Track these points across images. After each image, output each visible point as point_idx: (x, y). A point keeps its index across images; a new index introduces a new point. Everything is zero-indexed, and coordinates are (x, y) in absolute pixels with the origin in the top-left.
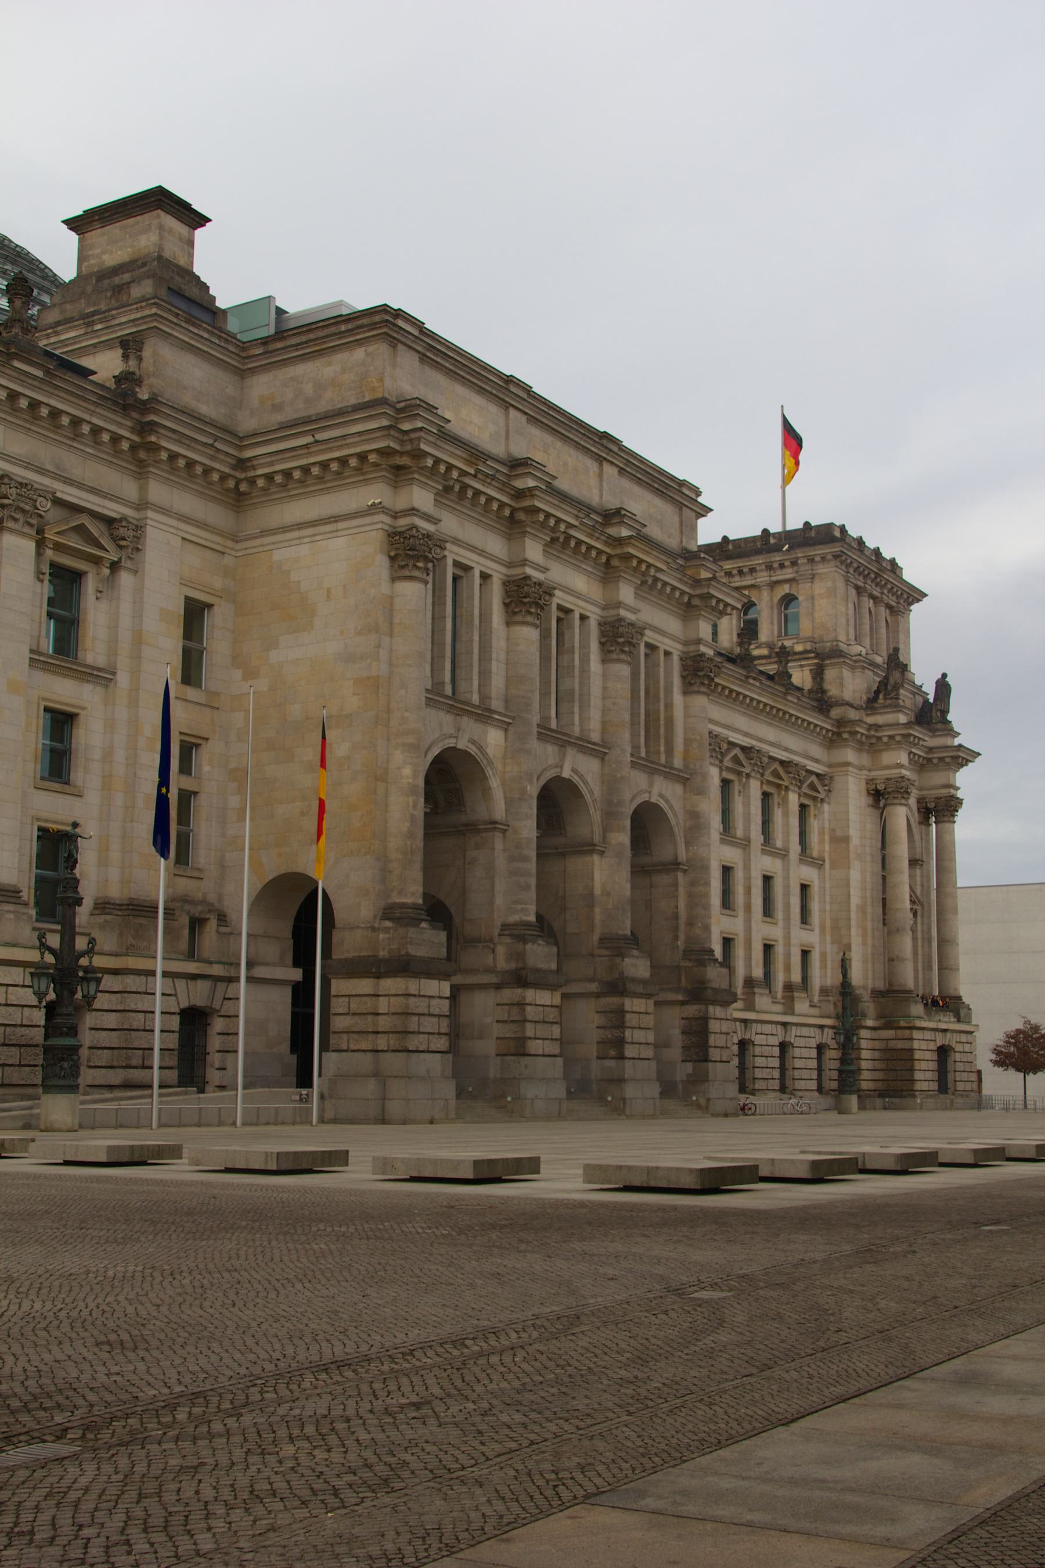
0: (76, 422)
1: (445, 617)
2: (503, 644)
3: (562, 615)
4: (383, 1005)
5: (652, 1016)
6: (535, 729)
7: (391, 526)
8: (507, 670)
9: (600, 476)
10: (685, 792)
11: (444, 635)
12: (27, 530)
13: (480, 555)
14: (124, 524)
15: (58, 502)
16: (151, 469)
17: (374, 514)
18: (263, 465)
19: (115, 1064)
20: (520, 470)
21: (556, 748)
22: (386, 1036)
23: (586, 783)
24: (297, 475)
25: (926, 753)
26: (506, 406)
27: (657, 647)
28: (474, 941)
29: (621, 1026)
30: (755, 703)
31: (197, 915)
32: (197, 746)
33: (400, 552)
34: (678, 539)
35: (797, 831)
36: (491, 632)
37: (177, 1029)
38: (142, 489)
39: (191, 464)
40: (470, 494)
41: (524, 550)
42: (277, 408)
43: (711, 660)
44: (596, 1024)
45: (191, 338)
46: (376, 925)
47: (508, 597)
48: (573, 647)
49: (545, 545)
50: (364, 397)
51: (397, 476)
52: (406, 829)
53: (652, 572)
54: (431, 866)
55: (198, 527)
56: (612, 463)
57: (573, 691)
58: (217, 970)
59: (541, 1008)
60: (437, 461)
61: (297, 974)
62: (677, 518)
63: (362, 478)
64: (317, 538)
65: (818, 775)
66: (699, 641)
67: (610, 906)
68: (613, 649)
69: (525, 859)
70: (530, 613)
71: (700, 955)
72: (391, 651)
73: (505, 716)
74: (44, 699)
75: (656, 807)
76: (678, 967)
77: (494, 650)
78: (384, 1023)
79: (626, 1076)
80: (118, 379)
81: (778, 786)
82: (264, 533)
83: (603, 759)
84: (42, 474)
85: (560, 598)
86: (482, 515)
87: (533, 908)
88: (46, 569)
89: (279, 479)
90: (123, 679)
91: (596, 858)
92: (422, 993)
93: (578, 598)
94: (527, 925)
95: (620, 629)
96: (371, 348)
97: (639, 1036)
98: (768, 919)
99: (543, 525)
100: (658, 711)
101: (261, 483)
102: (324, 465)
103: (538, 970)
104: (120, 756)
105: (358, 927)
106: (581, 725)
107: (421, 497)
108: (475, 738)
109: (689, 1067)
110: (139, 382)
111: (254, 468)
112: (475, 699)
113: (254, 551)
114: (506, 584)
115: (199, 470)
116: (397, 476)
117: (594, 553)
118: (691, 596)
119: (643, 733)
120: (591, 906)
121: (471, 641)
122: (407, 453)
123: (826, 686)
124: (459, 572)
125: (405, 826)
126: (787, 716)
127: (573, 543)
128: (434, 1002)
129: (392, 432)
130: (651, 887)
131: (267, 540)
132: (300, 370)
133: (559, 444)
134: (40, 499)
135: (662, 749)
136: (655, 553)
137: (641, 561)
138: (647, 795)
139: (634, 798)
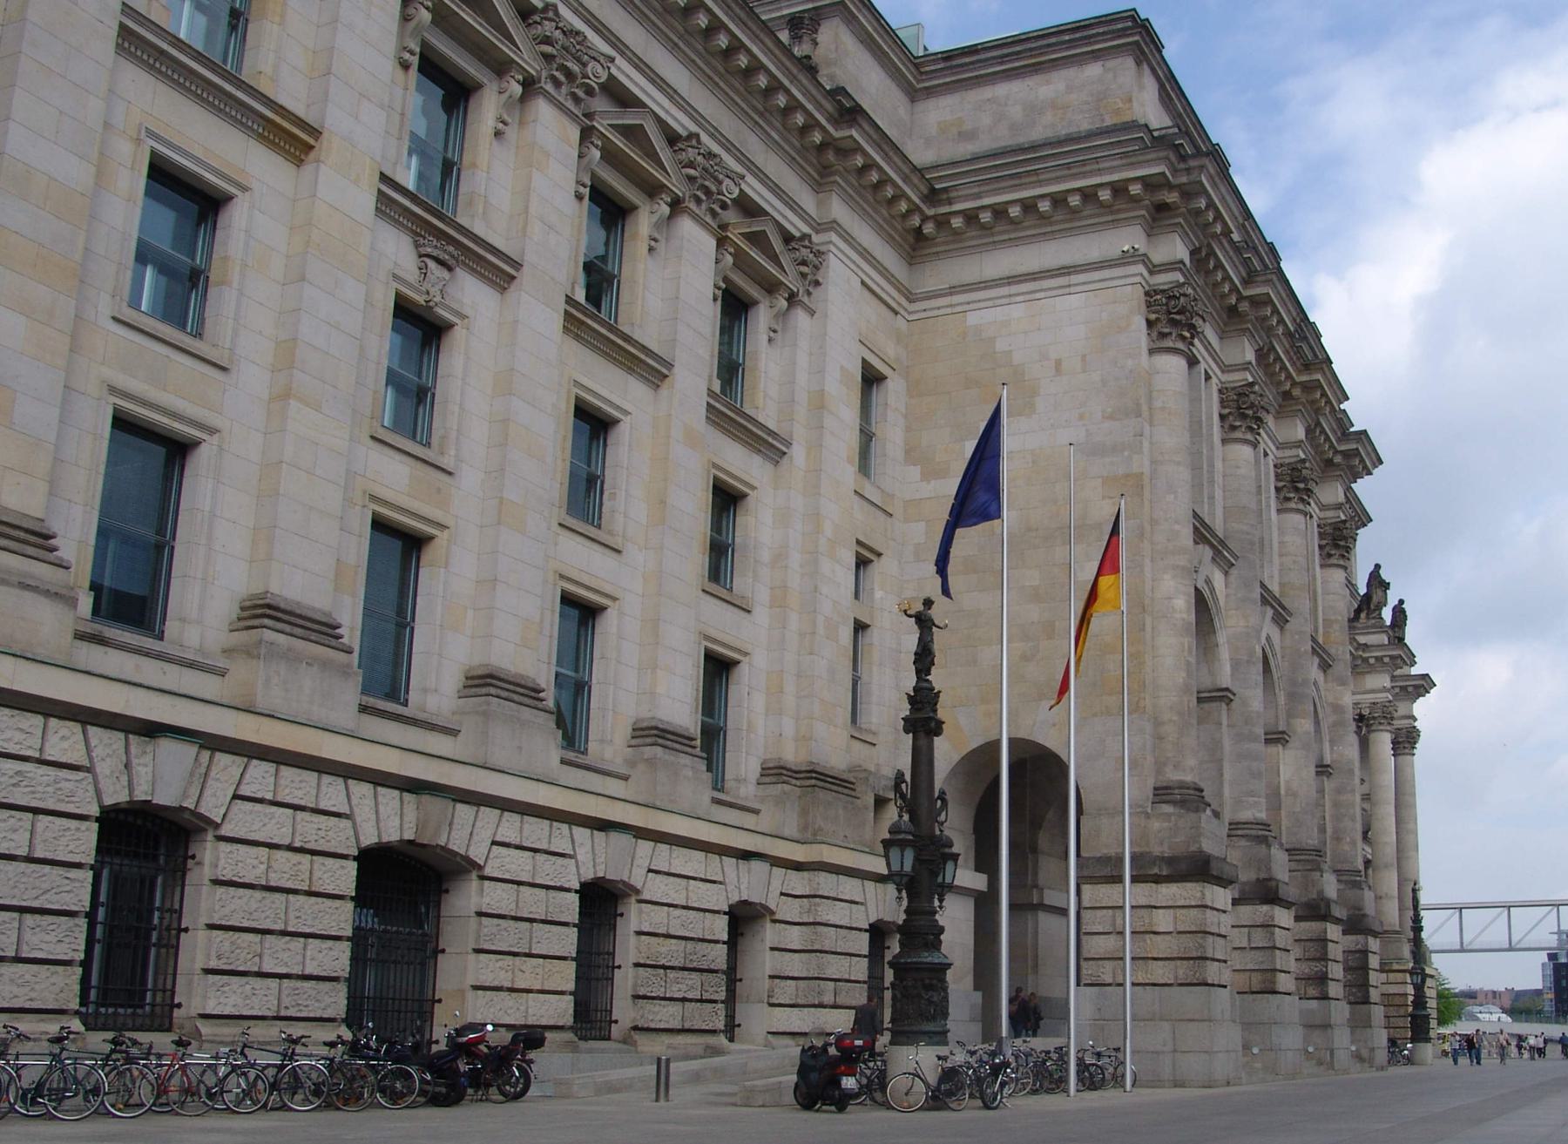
16: (838, 179)
17: (1128, 263)
18: (967, 198)
19: (800, 1001)
47: (1223, 407)
50: (1103, 120)
52: (1181, 680)
64: (1038, 295)
82: (953, 290)
89: (986, 217)
90: (798, 453)
95: (1304, 471)
96: (1111, 64)
104: (795, 559)
111: (950, 202)
113: (936, 313)
122: (1179, 187)
132: (1002, 90)
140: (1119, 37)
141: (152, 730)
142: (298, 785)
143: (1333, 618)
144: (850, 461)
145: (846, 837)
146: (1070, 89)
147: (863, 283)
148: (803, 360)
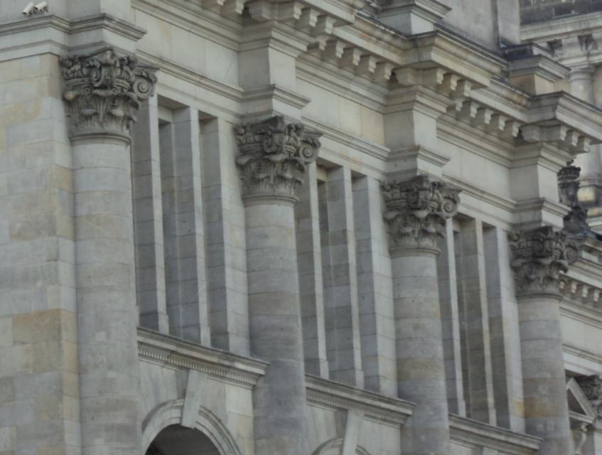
1: (151, 197)
8: (249, 282)
11: (152, 228)
13: (199, 84)
17: (36, 27)
27: (472, 219)
33: (82, 92)
34: (490, 23)
36: (220, 218)
41: (267, 71)
48: (345, 231)
49: (299, 59)
53: (329, 26)
57: (348, 308)
66: (539, 204)
72: (77, 265)
77: (227, 248)
83: (402, 428)
86: (198, 14)
93: (348, 144)
99: (298, 25)
100: (480, 333)
106: (364, 368)
108: (209, 407)
112: (205, 335)
117: (372, 65)
118: (523, 125)
121: (192, 234)
127: (339, 50)
135: (491, 400)
136: (471, 58)
137: (449, 73)
143: (537, 376)
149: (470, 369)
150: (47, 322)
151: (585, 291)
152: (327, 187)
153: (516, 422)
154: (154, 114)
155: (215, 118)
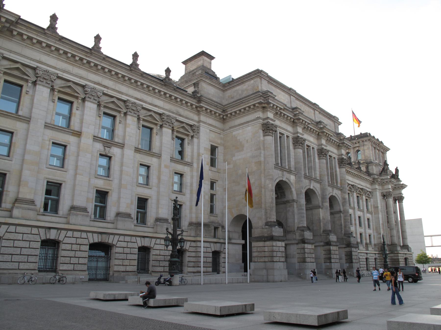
0: (181, 100)
2: (293, 154)
3: (308, 147)
4: (266, 249)
5: (338, 251)
6: (303, 176)
7: (262, 122)
8: (295, 160)
9: (315, 114)
10: (341, 193)
12: (169, 127)
13: (286, 131)
14: (194, 126)
15: (177, 121)
16: (201, 113)
18: (229, 111)
19: (195, 266)
20: (295, 110)
21: (309, 181)
22: (267, 258)
23: (317, 190)
24: (238, 112)
25: (395, 186)
26: (290, 95)
28: (289, 232)
29: (330, 254)
30: (354, 174)
31: (216, 226)
32: (215, 182)
35: (365, 205)
37: (211, 257)
38: (199, 118)
39: (211, 111)
40: (282, 115)
42: (232, 98)
43: (345, 159)
44: (323, 254)
45: (211, 82)
46: (264, 227)
47: (294, 142)
48: (311, 155)
51: (263, 110)
54: (277, 213)
55: (213, 127)
56: (317, 111)
57: (312, 166)
58: (222, 241)
59: (309, 249)
60: (274, 105)
61: (243, 242)
62: (334, 125)
63: (254, 111)
65: (369, 192)
66: (342, 155)
67: (325, 222)
68: (321, 156)
69: (303, 209)
70: (300, 145)
71: (349, 235)
73: (295, 172)
74: (174, 170)
75: (334, 196)
76: (343, 238)
78: (267, 254)
79: (332, 267)
80: (193, 93)
81: (360, 194)
82: (231, 128)
83: (320, 184)
84: (173, 113)
85: (307, 143)
86: (286, 121)
87: (305, 222)
88: (175, 137)
91: (320, 210)
92: (277, 246)
93: (311, 143)
94: (304, 227)
96: (255, 80)
97: (335, 256)
98: (360, 227)
99: (302, 123)
101: (229, 115)
102: (245, 109)
103: (308, 239)
105: (259, 228)
106: (314, 175)
107: (270, 115)
109: (348, 265)
110: (198, 93)
111: (227, 112)
112: (287, 167)
114: (293, 138)
115: (213, 113)
116: (263, 110)
117: (315, 131)
118: (339, 143)
119: (330, 178)
120: (320, 222)
121: (285, 153)
122: (266, 103)
123: (369, 171)
124: (281, 136)
125: (270, 200)
126: (361, 177)
128: (280, 248)
129: (262, 98)
130: (334, 218)
131: (231, 130)
132: (238, 88)
133: (304, 105)
134: (173, 119)
135: (335, 182)
137: (327, 133)
138: (332, 193)
139: (329, 194)
140: (255, 75)
141: (50, 228)
142: (77, 234)
144: (207, 164)
145: (206, 235)
146: (248, 86)
147: (210, 130)
148: (195, 147)
149: (332, 177)
150: (259, 163)
151: (352, 173)
152: (308, 149)
153: (339, 185)
154: (279, 135)
155: (289, 136)
